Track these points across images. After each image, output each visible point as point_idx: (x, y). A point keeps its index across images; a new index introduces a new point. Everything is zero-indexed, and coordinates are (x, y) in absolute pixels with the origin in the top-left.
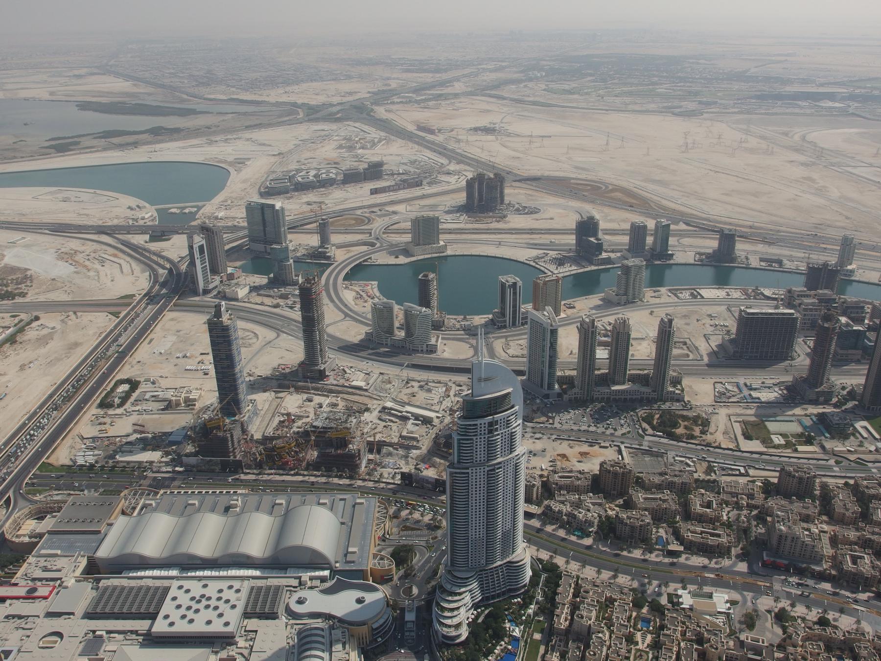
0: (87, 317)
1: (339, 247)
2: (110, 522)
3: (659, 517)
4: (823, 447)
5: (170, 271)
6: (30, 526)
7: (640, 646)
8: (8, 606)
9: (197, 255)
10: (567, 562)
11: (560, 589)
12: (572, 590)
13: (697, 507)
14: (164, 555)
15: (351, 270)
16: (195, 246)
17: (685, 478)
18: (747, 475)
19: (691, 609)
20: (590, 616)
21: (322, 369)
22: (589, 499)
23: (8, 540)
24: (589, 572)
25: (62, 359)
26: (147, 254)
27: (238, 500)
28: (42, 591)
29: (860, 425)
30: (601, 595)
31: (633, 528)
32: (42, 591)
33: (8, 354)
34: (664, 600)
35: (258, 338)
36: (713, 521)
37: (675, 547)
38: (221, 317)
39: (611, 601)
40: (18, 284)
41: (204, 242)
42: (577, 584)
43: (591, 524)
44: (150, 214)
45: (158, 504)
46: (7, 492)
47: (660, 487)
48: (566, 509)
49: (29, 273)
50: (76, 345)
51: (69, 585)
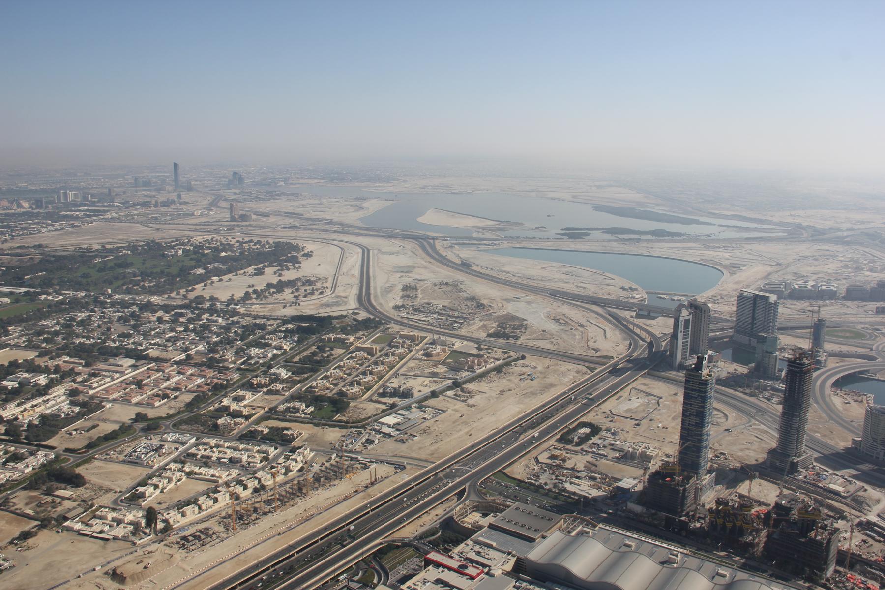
0: (565, 366)
1: (832, 354)
2: (545, 534)
5: (650, 345)
6: (475, 517)
8: (440, 572)
9: (681, 328)
14: (590, 579)
15: (842, 377)
16: (681, 319)
21: (795, 461)
23: (455, 521)
25: (536, 394)
26: (631, 327)
27: (677, 556)
28: (471, 571)
32: (471, 571)
33: (493, 380)
35: (727, 419)
38: (701, 370)
40: (514, 329)
41: (690, 317)
44: (640, 295)
45: (595, 534)
46: (464, 484)
49: (525, 322)
50: (552, 385)
51: (496, 574)
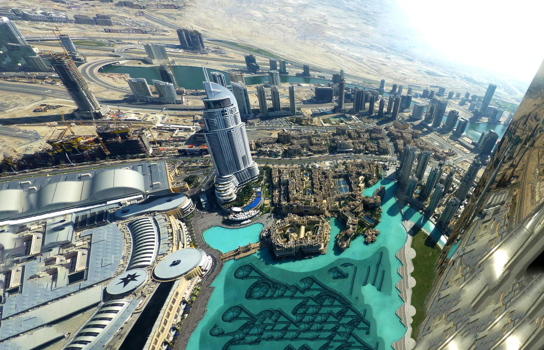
3: (303, 146)
4: (346, 123)
7: (306, 181)
10: (273, 165)
11: (273, 173)
12: (277, 172)
13: (315, 142)
17: (309, 134)
18: (327, 132)
19: (319, 167)
20: (286, 177)
22: (276, 145)
24: (283, 166)
29: (353, 117)
30: (289, 170)
31: (295, 151)
34: (310, 167)
36: (320, 144)
37: (310, 153)
39: (293, 172)
42: (279, 170)
43: (279, 152)
47: (301, 138)
48: (269, 149)
